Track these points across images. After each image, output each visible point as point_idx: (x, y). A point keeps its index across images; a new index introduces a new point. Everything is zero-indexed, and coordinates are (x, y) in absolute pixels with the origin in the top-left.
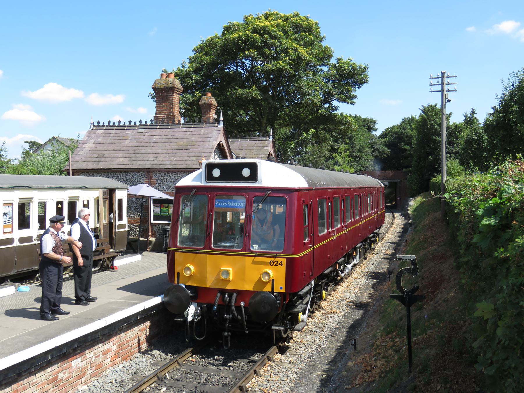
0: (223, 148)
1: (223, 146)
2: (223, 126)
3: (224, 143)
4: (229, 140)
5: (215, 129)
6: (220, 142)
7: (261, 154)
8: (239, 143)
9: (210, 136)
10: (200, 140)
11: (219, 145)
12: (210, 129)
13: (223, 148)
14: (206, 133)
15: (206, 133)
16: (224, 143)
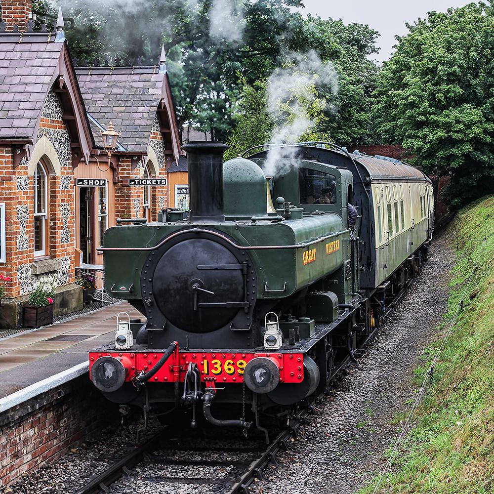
0: (65, 91)
1: (64, 85)
2: (65, 42)
3: (66, 79)
4: (77, 72)
5: (50, 47)
6: (59, 77)
7: (142, 105)
8: (88, 78)
9: (37, 62)
10: (11, 71)
11: (56, 84)
12: (35, 47)
13: (65, 91)
14: (26, 55)
15: (26, 55)
16: (66, 79)
